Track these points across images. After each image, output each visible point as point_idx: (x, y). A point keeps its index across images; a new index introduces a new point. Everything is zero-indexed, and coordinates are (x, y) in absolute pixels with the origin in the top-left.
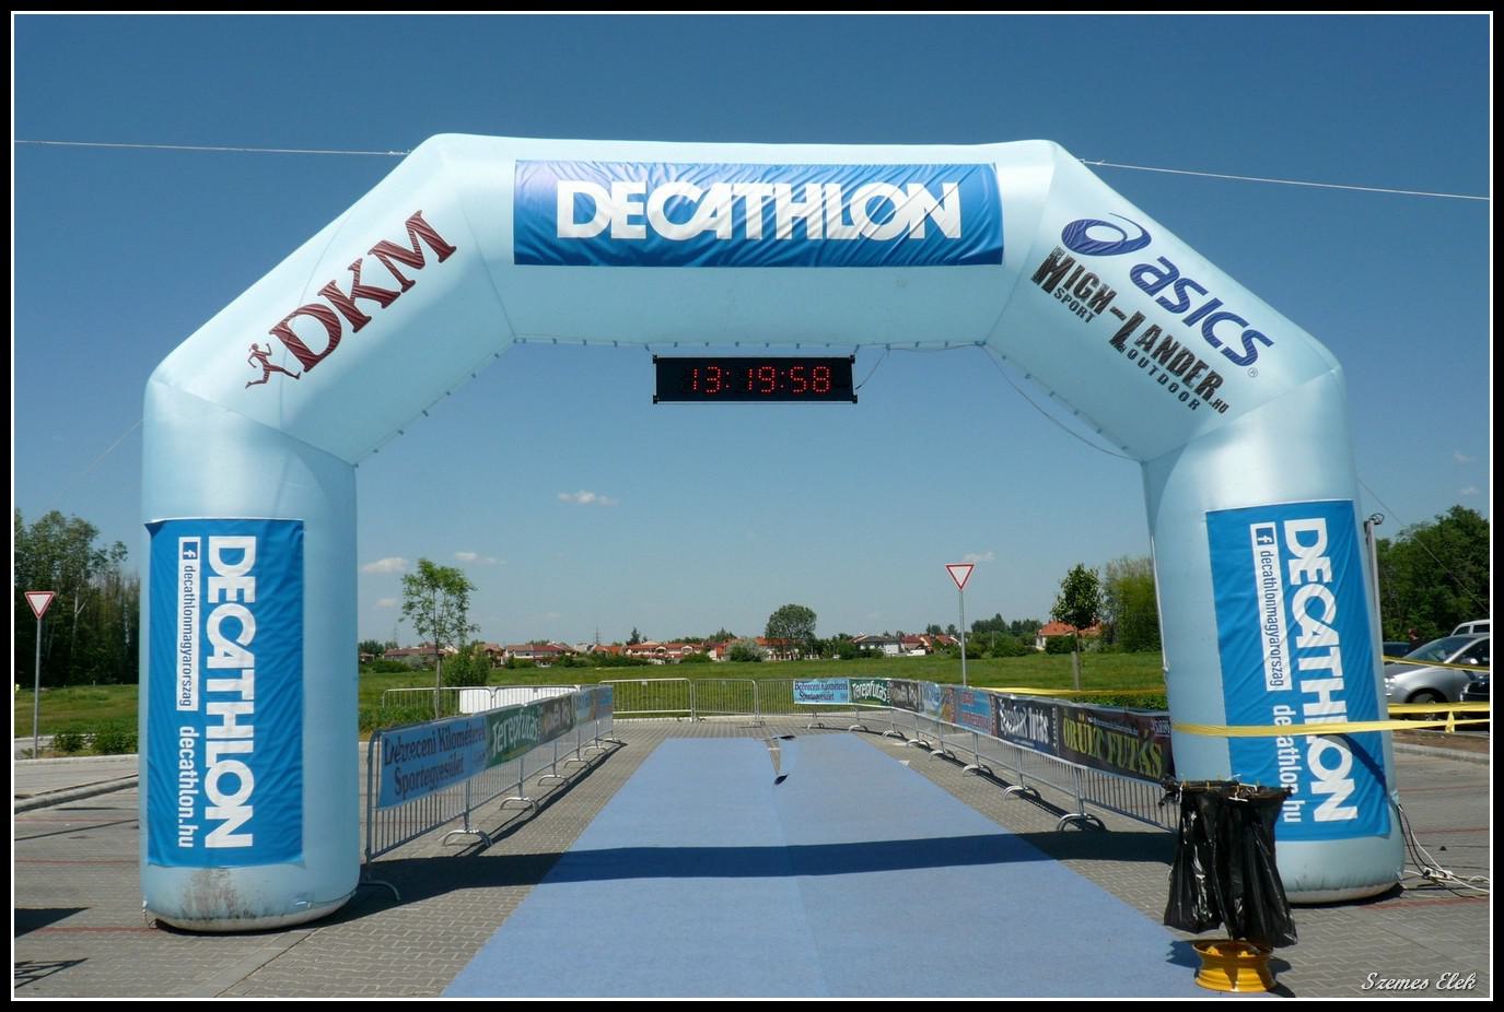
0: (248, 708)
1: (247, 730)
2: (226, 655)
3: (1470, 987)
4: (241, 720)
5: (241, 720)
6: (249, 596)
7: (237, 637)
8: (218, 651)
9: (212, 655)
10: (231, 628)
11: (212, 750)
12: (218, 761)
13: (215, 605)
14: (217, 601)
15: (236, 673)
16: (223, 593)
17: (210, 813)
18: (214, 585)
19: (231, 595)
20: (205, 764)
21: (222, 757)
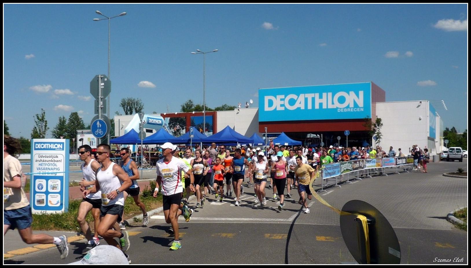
0: (317, 95)
2: (300, 103)
3: (462, 261)
4: (321, 97)
5: (321, 97)
6: (283, 97)
7: (294, 99)
9: (300, 108)
10: (292, 102)
11: (330, 106)
13: (285, 108)
14: (284, 107)
15: (306, 100)
16: (282, 105)
18: (279, 108)
19: (282, 102)
20: (336, 108)
21: (333, 103)
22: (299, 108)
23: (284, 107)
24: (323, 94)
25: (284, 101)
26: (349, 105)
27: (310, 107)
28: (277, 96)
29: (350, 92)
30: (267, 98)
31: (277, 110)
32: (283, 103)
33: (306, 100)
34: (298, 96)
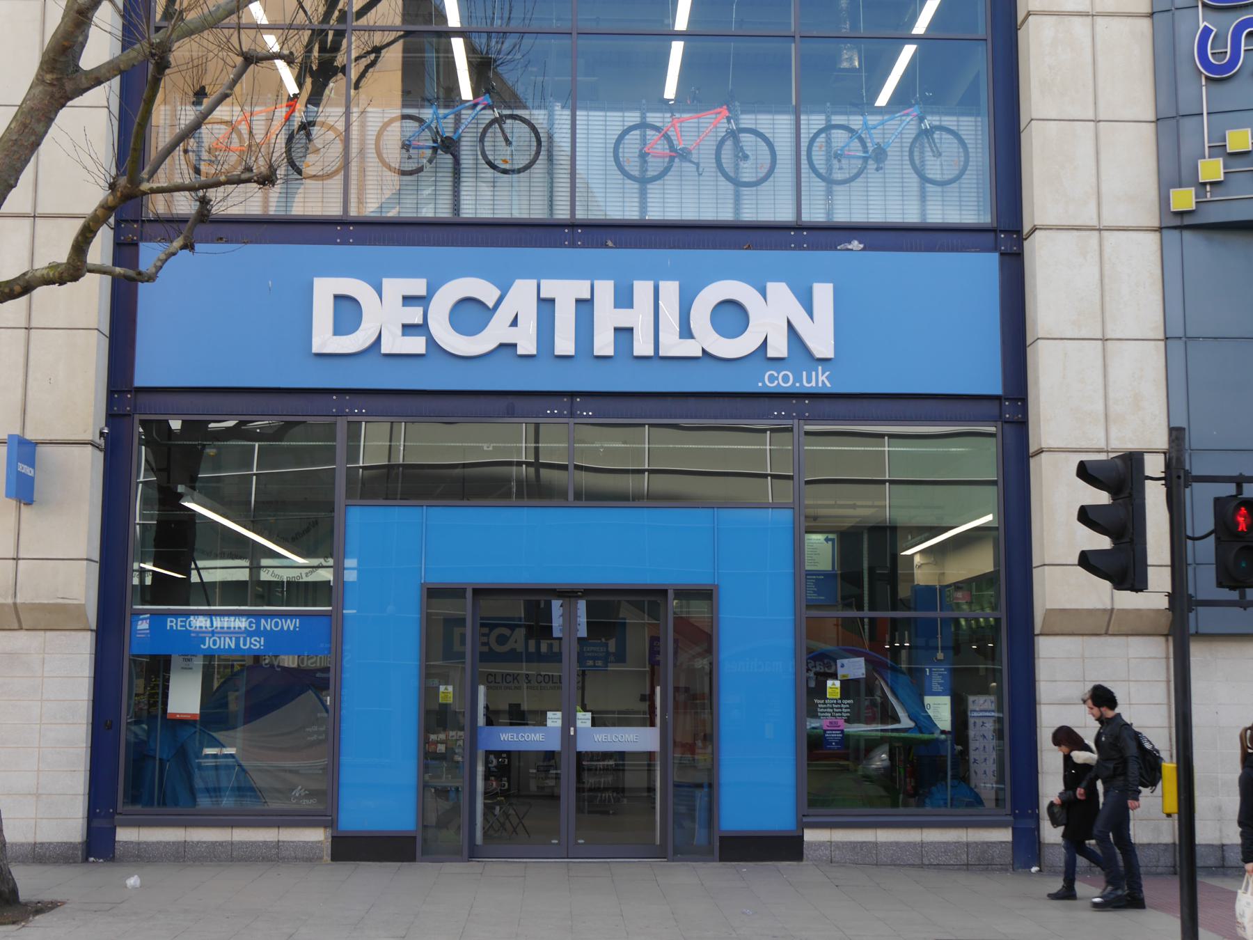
2: (514, 323)
4: (624, 299)
5: (624, 299)
6: (418, 286)
8: (509, 336)
11: (673, 345)
12: (691, 336)
13: (431, 343)
15: (546, 305)
16: (408, 329)
18: (394, 343)
19: (414, 315)
21: (686, 332)
27: (565, 344)
28: (387, 283)
29: (771, 286)
30: (325, 290)
31: (386, 348)
33: (546, 305)
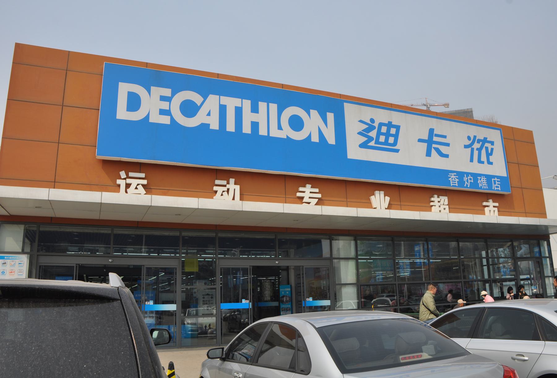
1: (262, 106)
2: (209, 114)
4: (255, 109)
5: (255, 109)
6: (167, 92)
8: (206, 120)
9: (209, 125)
11: (275, 133)
13: (172, 119)
14: (170, 117)
15: (223, 109)
16: (163, 112)
17: (315, 139)
18: (156, 118)
19: (165, 105)
21: (280, 128)
22: (204, 127)
23: (170, 117)
24: (260, 103)
25: (169, 103)
26: (310, 136)
27: (231, 127)
28: (153, 89)
31: (151, 120)
32: (168, 109)
33: (223, 109)
34: (205, 97)
